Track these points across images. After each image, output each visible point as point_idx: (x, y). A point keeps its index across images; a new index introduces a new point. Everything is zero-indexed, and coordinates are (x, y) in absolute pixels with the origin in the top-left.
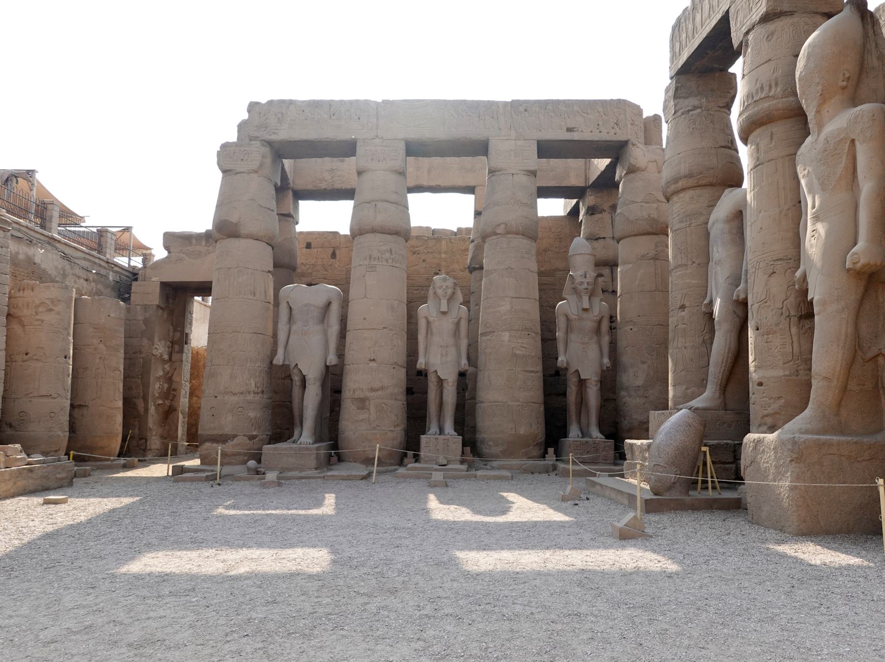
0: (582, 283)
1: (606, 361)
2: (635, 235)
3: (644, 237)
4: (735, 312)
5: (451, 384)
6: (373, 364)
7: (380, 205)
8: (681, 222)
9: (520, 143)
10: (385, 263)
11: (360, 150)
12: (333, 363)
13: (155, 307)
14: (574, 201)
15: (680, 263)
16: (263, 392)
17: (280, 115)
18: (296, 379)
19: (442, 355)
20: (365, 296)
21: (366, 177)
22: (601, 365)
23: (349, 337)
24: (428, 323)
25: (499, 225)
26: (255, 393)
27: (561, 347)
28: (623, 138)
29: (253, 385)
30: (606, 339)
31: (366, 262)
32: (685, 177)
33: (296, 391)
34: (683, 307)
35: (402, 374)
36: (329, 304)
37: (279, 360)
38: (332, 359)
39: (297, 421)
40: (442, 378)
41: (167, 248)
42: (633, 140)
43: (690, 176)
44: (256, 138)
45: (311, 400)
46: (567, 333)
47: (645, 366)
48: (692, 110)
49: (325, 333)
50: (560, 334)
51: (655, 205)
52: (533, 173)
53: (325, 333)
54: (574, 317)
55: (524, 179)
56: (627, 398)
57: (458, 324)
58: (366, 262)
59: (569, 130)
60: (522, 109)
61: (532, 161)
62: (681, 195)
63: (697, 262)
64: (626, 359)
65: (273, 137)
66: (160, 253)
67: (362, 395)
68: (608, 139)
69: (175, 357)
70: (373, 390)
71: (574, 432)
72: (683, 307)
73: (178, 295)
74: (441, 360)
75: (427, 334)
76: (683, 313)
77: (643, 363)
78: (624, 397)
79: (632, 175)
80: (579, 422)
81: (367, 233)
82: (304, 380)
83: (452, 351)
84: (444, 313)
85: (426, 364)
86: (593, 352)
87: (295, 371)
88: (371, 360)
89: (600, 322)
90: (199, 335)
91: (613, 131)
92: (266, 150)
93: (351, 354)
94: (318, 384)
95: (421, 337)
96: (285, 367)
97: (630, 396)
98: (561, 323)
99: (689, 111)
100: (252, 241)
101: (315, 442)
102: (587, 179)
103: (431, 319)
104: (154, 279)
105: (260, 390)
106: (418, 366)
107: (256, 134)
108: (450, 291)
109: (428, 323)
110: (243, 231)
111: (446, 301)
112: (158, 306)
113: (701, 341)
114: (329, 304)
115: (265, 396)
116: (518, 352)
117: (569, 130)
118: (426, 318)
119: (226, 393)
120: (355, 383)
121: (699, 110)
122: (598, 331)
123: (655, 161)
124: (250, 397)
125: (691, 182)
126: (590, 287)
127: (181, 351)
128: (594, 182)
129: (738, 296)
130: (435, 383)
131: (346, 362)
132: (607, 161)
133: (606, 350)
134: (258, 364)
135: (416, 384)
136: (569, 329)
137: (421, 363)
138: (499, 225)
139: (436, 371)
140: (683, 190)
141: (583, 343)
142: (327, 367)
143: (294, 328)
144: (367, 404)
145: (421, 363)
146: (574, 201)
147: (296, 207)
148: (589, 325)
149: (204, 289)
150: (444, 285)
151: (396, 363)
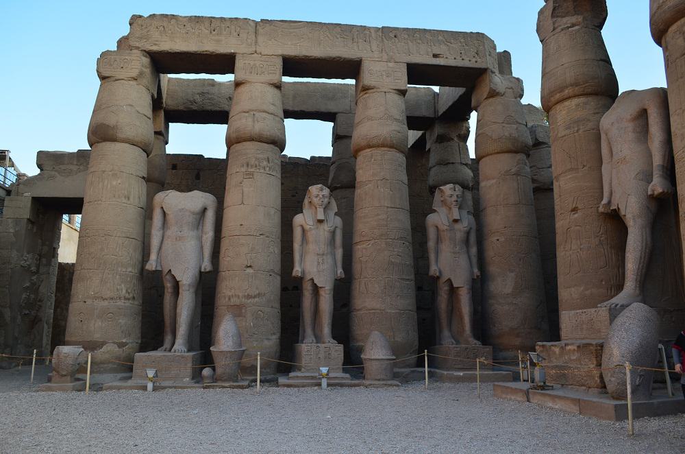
0: (451, 196)
1: (476, 271)
2: (498, 153)
3: (506, 155)
4: (648, 208)
5: (328, 292)
6: (249, 271)
7: (257, 114)
8: (568, 128)
9: (391, 65)
10: (262, 171)
11: (239, 64)
12: (207, 270)
13: (26, 220)
14: (420, 133)
15: (569, 167)
16: (134, 298)
17: (162, 28)
18: (168, 285)
19: (319, 263)
20: (243, 203)
21: (242, 89)
22: (472, 273)
23: (225, 244)
24: (304, 231)
26: (126, 299)
27: (432, 256)
28: (483, 66)
29: (124, 291)
30: (474, 250)
31: (243, 169)
32: (572, 85)
33: (168, 298)
34: (575, 210)
35: (277, 281)
36: (205, 210)
37: (152, 265)
38: (207, 266)
39: (168, 329)
40: (319, 285)
41: (39, 166)
42: (490, 67)
43: (576, 84)
44: (137, 48)
45: (185, 308)
46: (437, 243)
47: (513, 274)
48: (570, 27)
49: (200, 239)
51: (515, 126)
52: (403, 93)
53: (200, 239)
54: (446, 227)
55: (396, 98)
56: (496, 306)
57: (333, 233)
58: (243, 169)
59: (435, 56)
60: (392, 35)
61: (402, 81)
62: (567, 103)
63: (588, 166)
64: (493, 269)
65: (155, 48)
66: (32, 170)
68: (471, 66)
69: (42, 270)
70: (249, 297)
71: (447, 340)
72: (575, 210)
73: (50, 211)
74: (316, 266)
75: (303, 239)
76: (576, 215)
79: (491, 99)
80: (450, 330)
81: (245, 141)
82: (176, 285)
83: (329, 260)
84: (320, 221)
85: (303, 272)
86: (463, 261)
87: (168, 277)
89: (468, 233)
90: (67, 252)
91: (474, 60)
92: (146, 60)
93: (226, 260)
94: (192, 290)
95: (297, 246)
96: (157, 274)
99: (568, 28)
100: (127, 145)
101: (189, 351)
102: (436, 111)
103: (307, 227)
104: (26, 194)
105: (131, 295)
106: (294, 274)
107: (137, 45)
108: (326, 200)
109: (304, 231)
110: (120, 135)
111: (322, 210)
112: (28, 219)
113: (597, 243)
114: (205, 210)
115: (136, 303)
116: (393, 260)
117: (435, 56)
118: (302, 226)
119: (96, 298)
120: (231, 289)
121: (577, 27)
122: (467, 242)
123: (512, 88)
124: (120, 303)
125: (577, 90)
126: (459, 200)
127: (49, 264)
128: (444, 112)
129: (653, 191)
130: (311, 292)
131: (221, 269)
132: (460, 91)
133: (474, 260)
134: (130, 269)
135: (291, 289)
137: (297, 270)
139: (312, 280)
140: (569, 98)
141: (454, 253)
142: (200, 272)
143: (169, 233)
144: (243, 311)
145: (297, 270)
146: (420, 133)
147: (167, 128)
148: (459, 236)
149: (74, 205)
150: (321, 194)
151: (272, 271)
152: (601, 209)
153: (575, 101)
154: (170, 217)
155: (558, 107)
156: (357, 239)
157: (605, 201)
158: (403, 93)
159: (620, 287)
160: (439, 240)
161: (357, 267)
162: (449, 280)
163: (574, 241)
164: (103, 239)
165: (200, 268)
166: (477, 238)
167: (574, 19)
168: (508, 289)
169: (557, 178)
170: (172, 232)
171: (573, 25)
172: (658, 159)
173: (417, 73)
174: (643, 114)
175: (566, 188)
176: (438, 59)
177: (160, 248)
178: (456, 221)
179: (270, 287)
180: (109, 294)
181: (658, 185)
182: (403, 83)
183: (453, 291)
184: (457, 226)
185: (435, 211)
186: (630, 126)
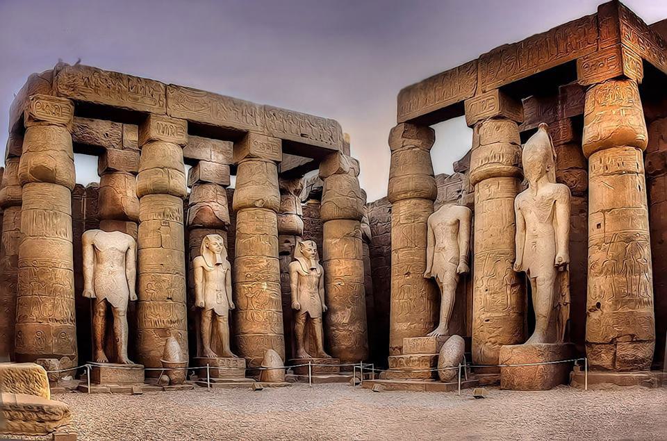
10: (175, 220)
15: (406, 245)
23: (145, 281)
25: (258, 200)
32: (412, 191)
50: (294, 286)
52: (277, 163)
59: (302, 135)
67: (163, 326)
70: (172, 322)
72: (408, 274)
77: (349, 308)
78: (334, 330)
84: (218, 264)
88: (168, 298)
91: (330, 142)
97: (338, 329)
98: (294, 277)
121: (418, 149)
136: (300, 282)
137: (200, 301)
138: (258, 200)
148: (315, 280)
152: (425, 276)
153: (413, 201)
154: (104, 254)
155: (402, 203)
156: (241, 278)
157: (428, 271)
158: (277, 163)
159: (435, 323)
160: (300, 282)
161: (243, 301)
162: (307, 314)
163: (406, 294)
164: (51, 270)
165: (129, 297)
166: (325, 280)
167: (416, 142)
168: (346, 321)
169: (396, 251)
170: (106, 267)
171: (416, 147)
172: (463, 252)
173: (289, 147)
174: (458, 221)
175: (400, 258)
176: (304, 138)
177: (94, 279)
178: (312, 269)
179: (180, 313)
180: (58, 316)
181: (462, 268)
182: (278, 156)
183: (308, 318)
184: (313, 273)
185: (296, 260)
186: (450, 228)
